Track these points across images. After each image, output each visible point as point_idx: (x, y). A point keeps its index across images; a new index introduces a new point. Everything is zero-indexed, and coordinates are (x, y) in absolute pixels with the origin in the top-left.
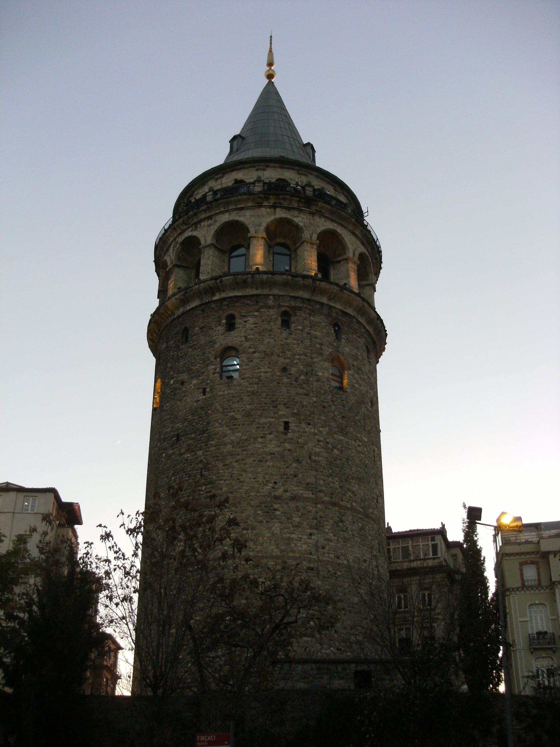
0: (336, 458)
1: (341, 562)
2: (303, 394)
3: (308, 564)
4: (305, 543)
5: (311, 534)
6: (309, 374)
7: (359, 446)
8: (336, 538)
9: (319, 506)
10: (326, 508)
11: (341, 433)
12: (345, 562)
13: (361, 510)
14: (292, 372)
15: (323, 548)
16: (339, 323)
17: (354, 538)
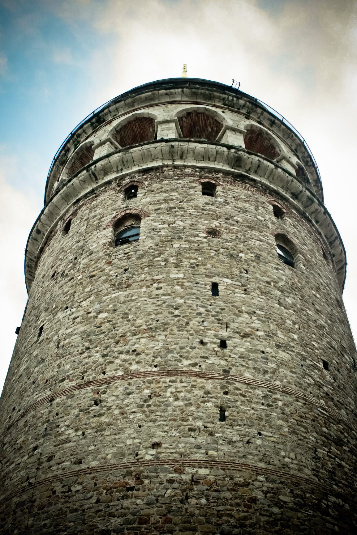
0: (101, 323)
1: (83, 466)
2: (66, 283)
3: (18, 499)
4: (23, 469)
5: (35, 448)
6: (78, 257)
7: (157, 289)
8: (80, 433)
9: (58, 400)
10: (68, 397)
11: (118, 289)
12: (94, 464)
13: (155, 369)
14: (59, 271)
15: (50, 459)
16: (135, 184)
17: (126, 418)
